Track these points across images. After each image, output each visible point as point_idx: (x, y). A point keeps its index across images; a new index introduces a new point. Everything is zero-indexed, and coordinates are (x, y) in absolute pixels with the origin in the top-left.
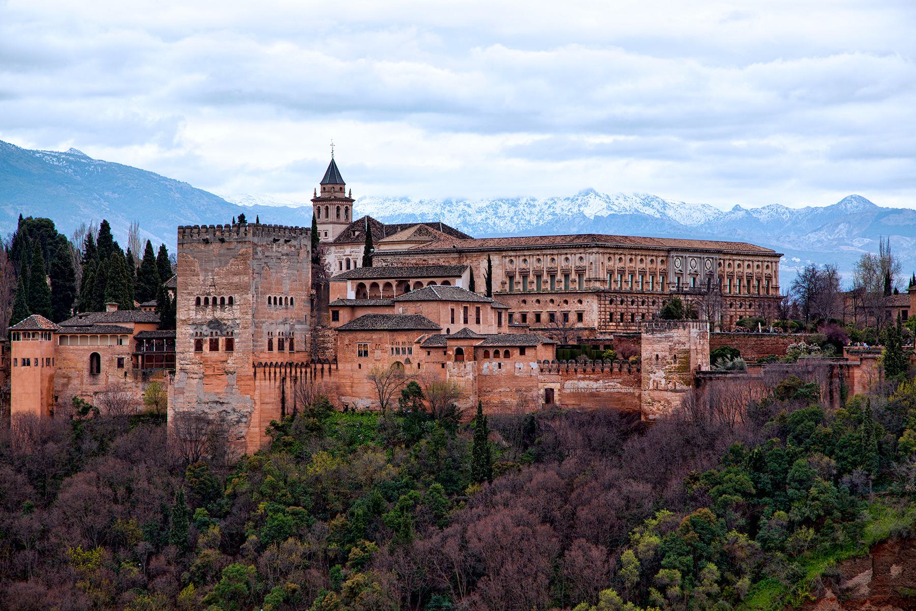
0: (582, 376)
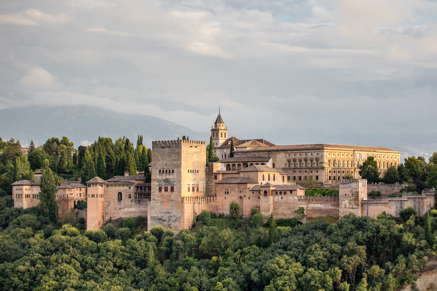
0: (315, 202)
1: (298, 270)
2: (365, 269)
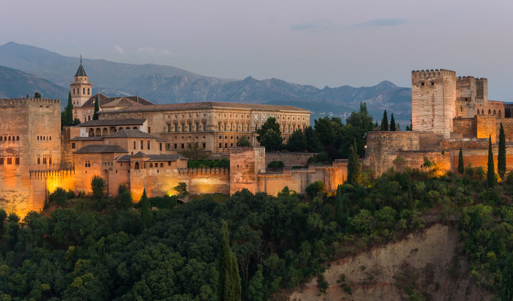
0: (200, 176)
1: (177, 262)
2: (261, 259)
